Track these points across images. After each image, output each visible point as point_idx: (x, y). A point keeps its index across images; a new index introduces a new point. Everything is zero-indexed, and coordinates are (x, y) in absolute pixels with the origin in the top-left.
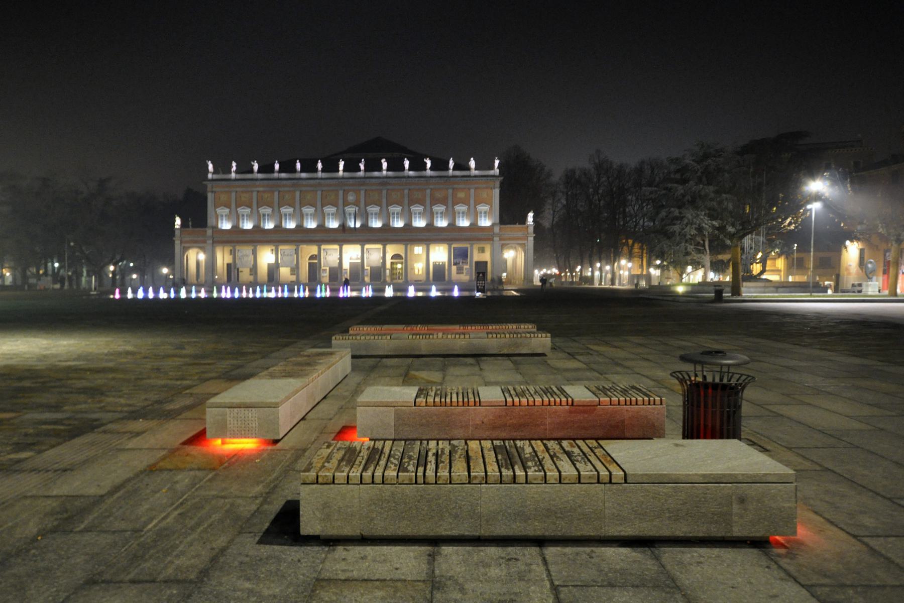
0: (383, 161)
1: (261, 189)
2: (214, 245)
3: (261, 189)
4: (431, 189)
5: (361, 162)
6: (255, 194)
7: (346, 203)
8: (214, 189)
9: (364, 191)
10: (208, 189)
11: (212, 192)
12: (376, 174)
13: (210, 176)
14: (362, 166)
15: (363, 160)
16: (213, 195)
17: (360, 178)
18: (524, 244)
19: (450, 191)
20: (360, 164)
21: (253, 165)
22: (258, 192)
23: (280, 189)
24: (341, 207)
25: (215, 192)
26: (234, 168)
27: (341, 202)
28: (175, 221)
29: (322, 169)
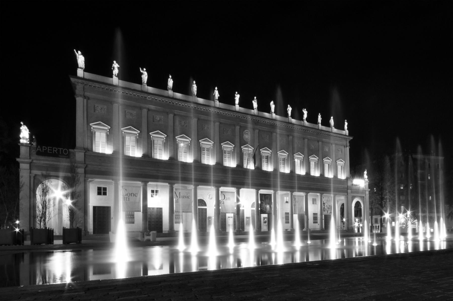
0: (272, 103)
1: (152, 107)
2: (87, 176)
3: (152, 107)
4: (308, 139)
5: (253, 99)
6: (145, 111)
7: (243, 143)
8: (87, 94)
9: (257, 131)
10: (77, 92)
11: (85, 97)
12: (266, 115)
13: (80, 73)
14: (255, 104)
15: (255, 98)
16: (85, 100)
17: (254, 115)
18: (364, 197)
19: (320, 143)
20: (253, 102)
21: (142, 74)
22: (149, 110)
23: (176, 112)
24: (238, 144)
25: (88, 98)
26: (116, 72)
27: (237, 140)
28: (19, 131)
29: (219, 97)
